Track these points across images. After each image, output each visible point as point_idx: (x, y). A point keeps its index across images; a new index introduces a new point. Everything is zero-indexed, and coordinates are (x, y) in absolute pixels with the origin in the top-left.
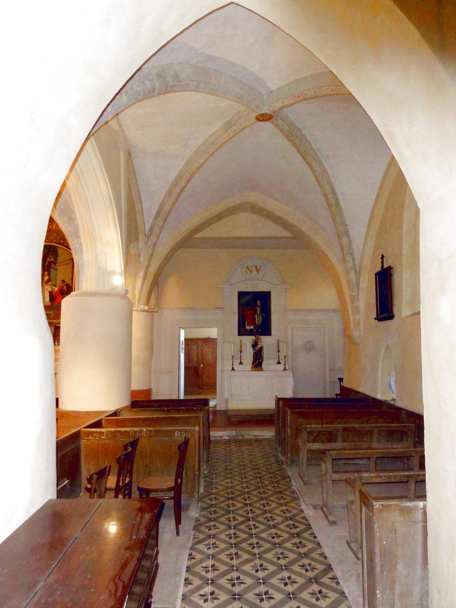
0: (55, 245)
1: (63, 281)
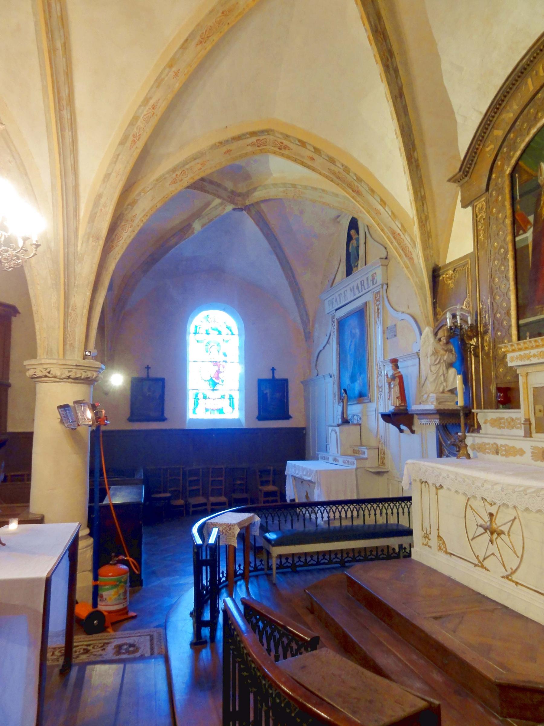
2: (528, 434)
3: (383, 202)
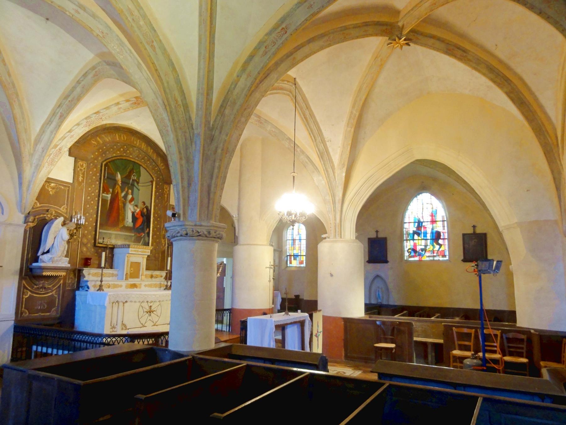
1: (144, 203)
2: (126, 279)
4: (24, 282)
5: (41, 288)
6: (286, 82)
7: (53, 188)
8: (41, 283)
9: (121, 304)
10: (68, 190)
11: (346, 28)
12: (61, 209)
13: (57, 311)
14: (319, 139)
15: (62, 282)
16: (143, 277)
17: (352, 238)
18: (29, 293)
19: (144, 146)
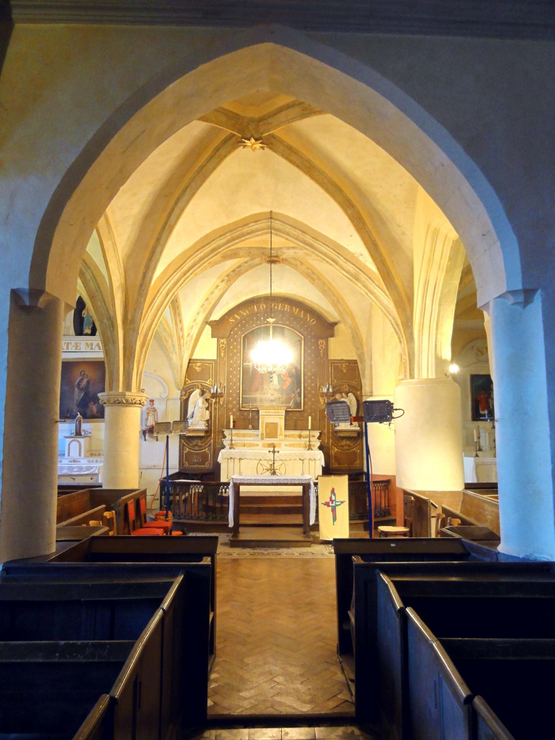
0: (282, 326)
2: (262, 439)
3: (180, 321)
4: (183, 441)
5: (196, 445)
6: (254, 224)
7: (199, 367)
8: (195, 443)
9: (237, 461)
10: (212, 366)
11: (203, 167)
12: (208, 382)
13: (210, 464)
14: (341, 261)
15: (212, 441)
16: (282, 437)
17: (430, 377)
18: (188, 449)
19: (287, 307)
